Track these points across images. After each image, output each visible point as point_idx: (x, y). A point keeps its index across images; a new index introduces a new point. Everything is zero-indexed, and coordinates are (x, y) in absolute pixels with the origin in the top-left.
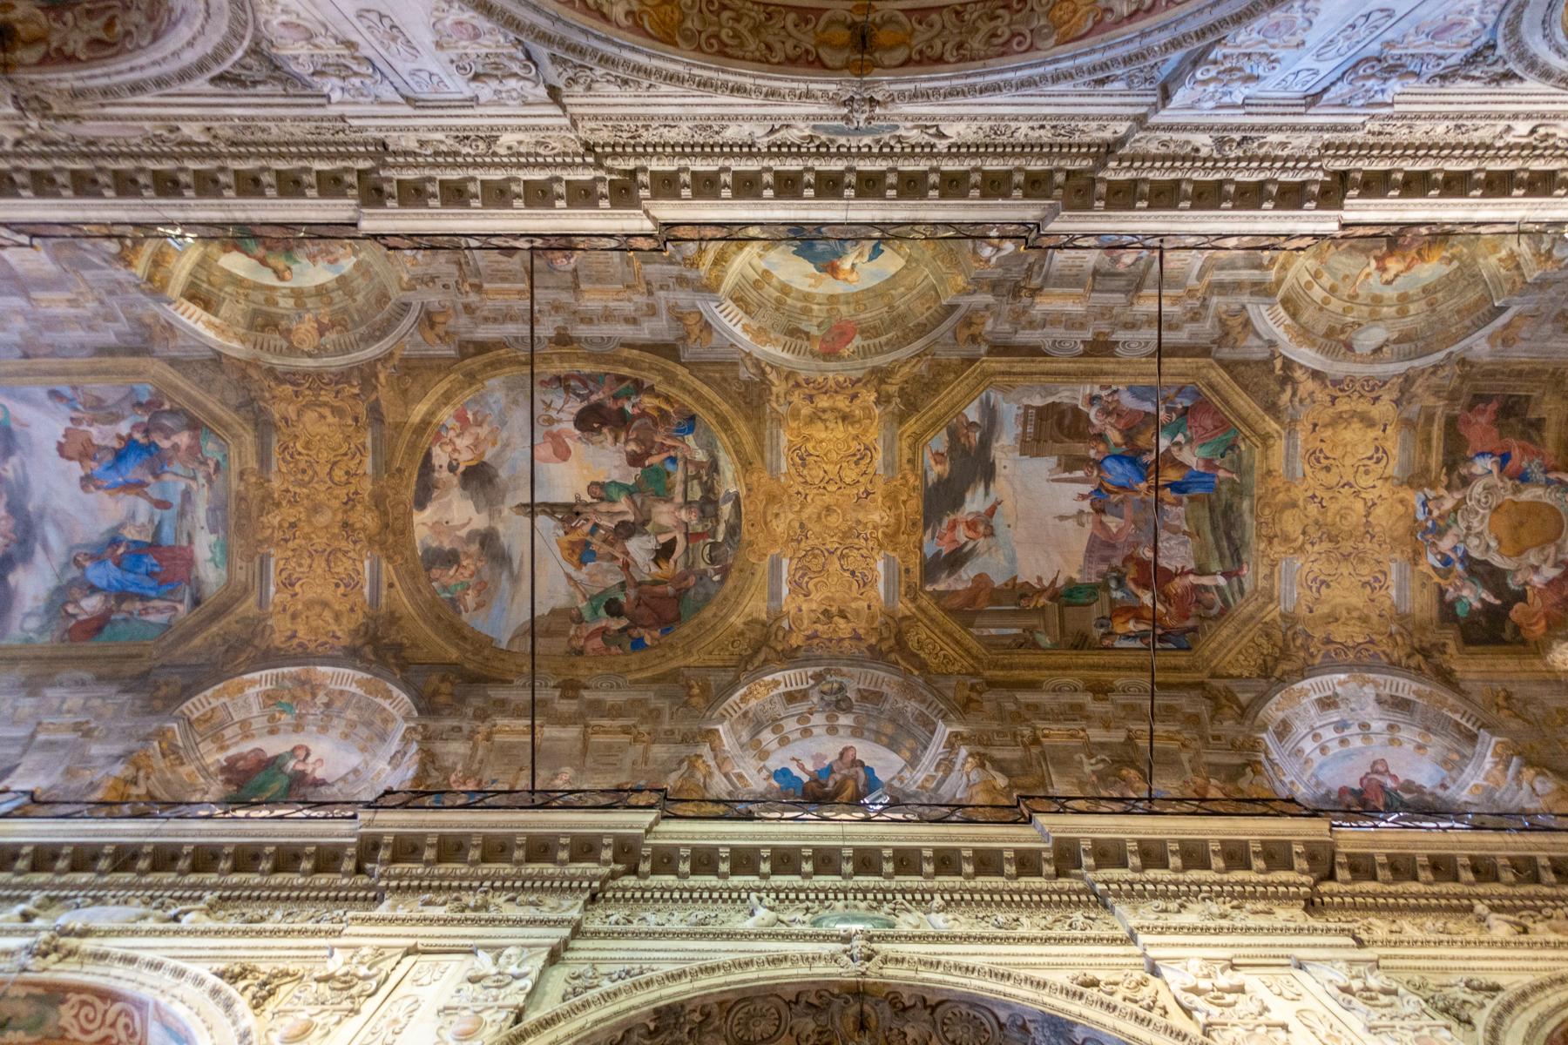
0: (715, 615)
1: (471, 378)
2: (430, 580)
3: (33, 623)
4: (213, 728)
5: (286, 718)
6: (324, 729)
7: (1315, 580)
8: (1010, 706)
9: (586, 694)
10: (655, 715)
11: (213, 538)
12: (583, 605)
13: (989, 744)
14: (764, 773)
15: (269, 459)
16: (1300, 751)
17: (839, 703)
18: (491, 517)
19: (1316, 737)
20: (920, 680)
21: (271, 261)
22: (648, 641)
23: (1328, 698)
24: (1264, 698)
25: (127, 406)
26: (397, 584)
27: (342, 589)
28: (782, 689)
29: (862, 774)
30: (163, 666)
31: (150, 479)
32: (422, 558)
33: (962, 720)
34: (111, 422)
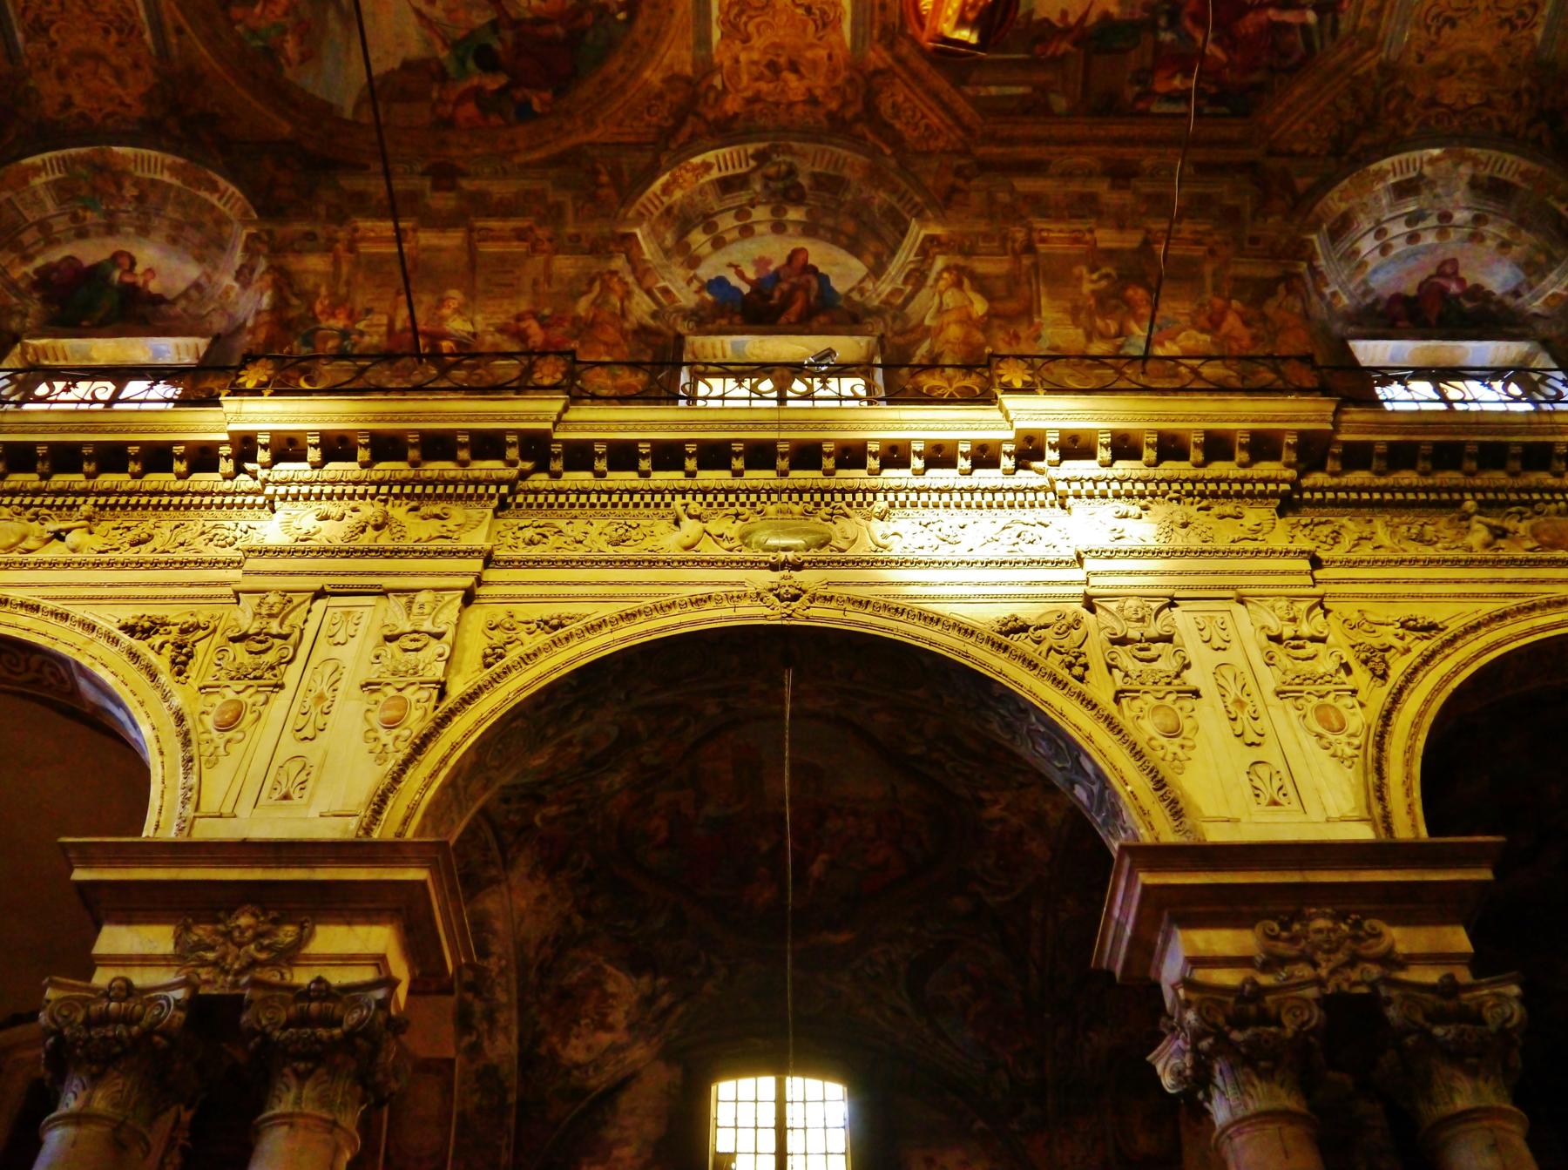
0: (622, 70)
2: (232, 23)
5: (91, 217)
6: (144, 231)
7: (1437, 16)
8: (1003, 197)
9: (465, 184)
10: (554, 214)
12: (444, 54)
13: (969, 253)
14: (695, 285)
16: (1356, 253)
17: (785, 192)
19: (1380, 233)
20: (893, 162)
22: (537, 106)
23: (1410, 181)
24: (1328, 183)
26: (188, 29)
27: (114, 38)
28: (715, 174)
29: (815, 284)
33: (941, 219)
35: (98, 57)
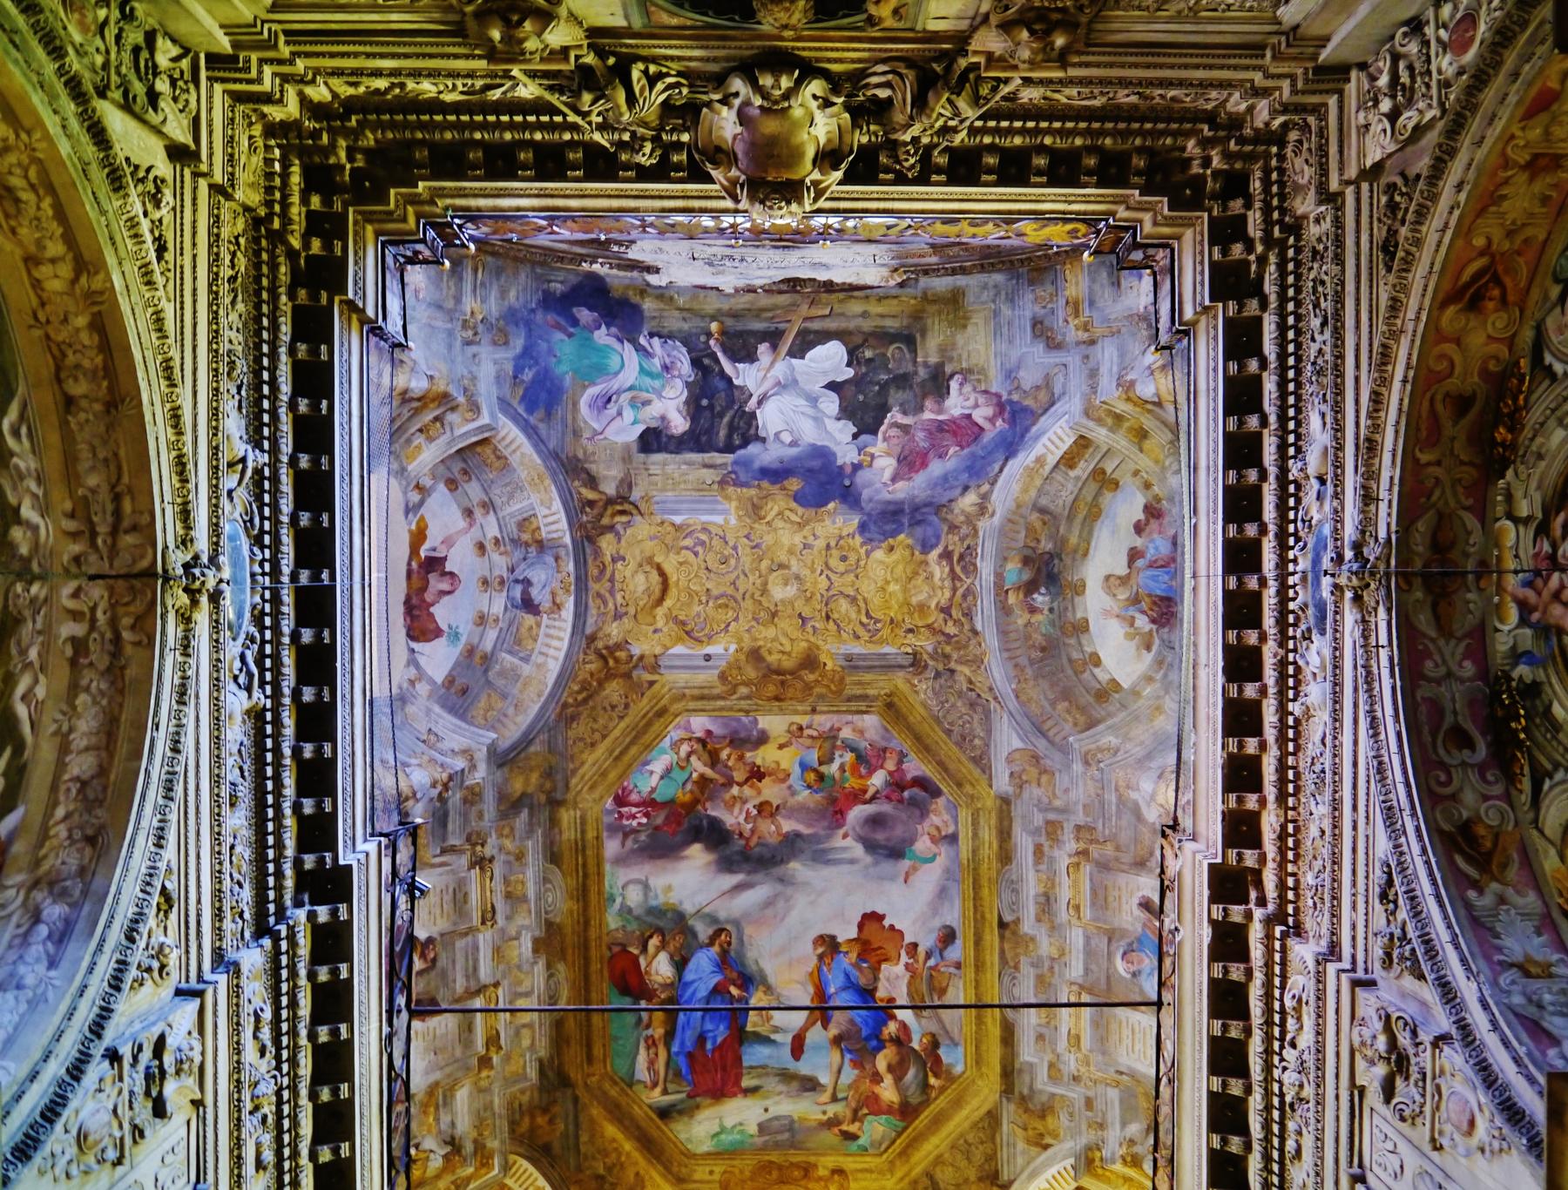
3: (634, 897)
11: (753, 1129)
25: (933, 1027)
30: (576, 1100)
31: (833, 1031)
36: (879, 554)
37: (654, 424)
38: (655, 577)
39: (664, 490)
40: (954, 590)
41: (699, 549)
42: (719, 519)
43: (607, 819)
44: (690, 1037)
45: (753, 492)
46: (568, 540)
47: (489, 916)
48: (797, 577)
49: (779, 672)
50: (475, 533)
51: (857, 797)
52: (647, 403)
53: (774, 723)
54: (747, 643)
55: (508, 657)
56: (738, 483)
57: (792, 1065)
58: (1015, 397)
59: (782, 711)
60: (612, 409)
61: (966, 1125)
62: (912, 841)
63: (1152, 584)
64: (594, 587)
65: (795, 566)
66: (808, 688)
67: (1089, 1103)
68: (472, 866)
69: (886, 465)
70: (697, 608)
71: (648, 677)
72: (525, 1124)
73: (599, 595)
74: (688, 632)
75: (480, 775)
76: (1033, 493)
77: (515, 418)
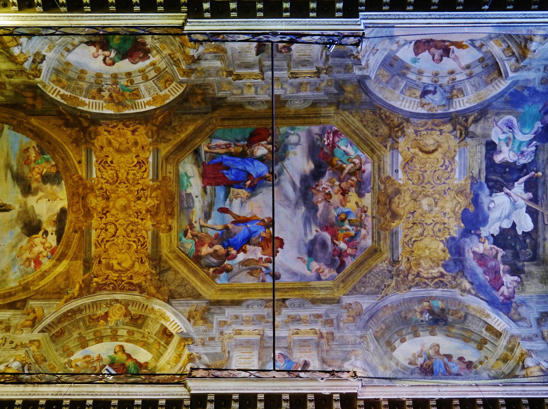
1: (25, 288)
2: (56, 165)
3: (293, 139)
4: (163, 78)
5: (123, 82)
6: (99, 76)
11: (189, 191)
15: (153, 239)
18: (25, 203)
21: (125, 357)
25: (235, 270)
27: (109, 160)
30: (206, 113)
31: (230, 226)
32: (62, 179)
34: (249, 260)
35: (118, 151)
36: (442, 246)
37: (498, 148)
38: (432, 148)
39: (470, 152)
40: (428, 279)
41: (444, 167)
42: (457, 176)
43: (328, 127)
44: (229, 163)
45: (468, 191)
46: (452, 110)
47: (294, 75)
48: (431, 210)
49: (390, 202)
50: (459, 70)
51: (334, 237)
52: (507, 145)
53: (368, 200)
54: (403, 188)
55: (404, 84)
56: (472, 184)
57: (216, 207)
58: (514, 305)
59: (373, 204)
60: (506, 129)
61: (194, 285)
62: (316, 260)
63: (438, 364)
64: (430, 122)
65: (436, 209)
66: (384, 215)
67: (212, 339)
68: (318, 68)
69: (480, 248)
70: (418, 166)
71: (389, 145)
72: (199, 91)
73: (426, 124)
74: (408, 162)
75: (357, 72)
76: (473, 313)
77: (509, 87)
